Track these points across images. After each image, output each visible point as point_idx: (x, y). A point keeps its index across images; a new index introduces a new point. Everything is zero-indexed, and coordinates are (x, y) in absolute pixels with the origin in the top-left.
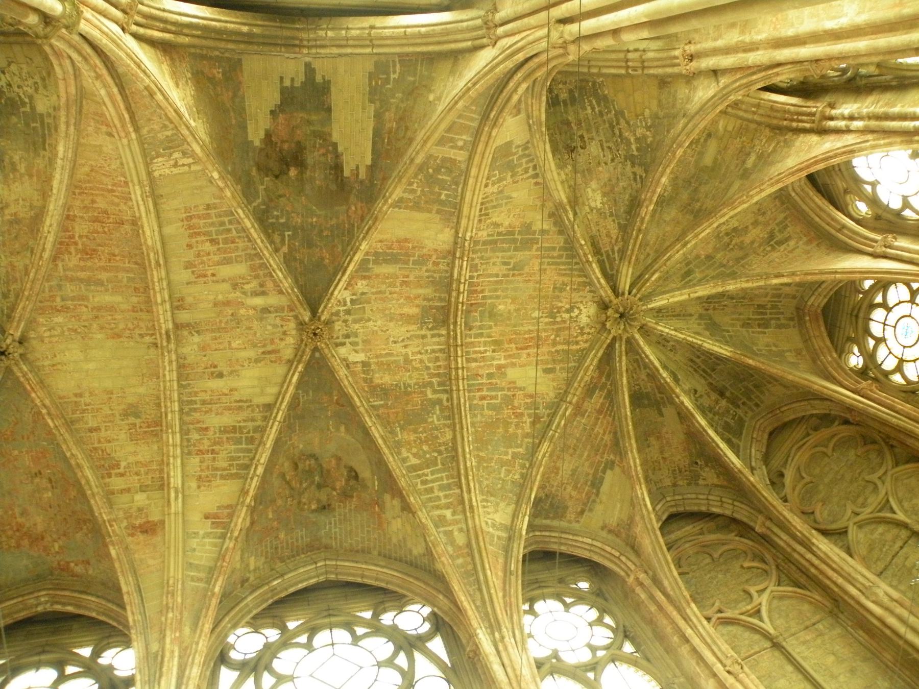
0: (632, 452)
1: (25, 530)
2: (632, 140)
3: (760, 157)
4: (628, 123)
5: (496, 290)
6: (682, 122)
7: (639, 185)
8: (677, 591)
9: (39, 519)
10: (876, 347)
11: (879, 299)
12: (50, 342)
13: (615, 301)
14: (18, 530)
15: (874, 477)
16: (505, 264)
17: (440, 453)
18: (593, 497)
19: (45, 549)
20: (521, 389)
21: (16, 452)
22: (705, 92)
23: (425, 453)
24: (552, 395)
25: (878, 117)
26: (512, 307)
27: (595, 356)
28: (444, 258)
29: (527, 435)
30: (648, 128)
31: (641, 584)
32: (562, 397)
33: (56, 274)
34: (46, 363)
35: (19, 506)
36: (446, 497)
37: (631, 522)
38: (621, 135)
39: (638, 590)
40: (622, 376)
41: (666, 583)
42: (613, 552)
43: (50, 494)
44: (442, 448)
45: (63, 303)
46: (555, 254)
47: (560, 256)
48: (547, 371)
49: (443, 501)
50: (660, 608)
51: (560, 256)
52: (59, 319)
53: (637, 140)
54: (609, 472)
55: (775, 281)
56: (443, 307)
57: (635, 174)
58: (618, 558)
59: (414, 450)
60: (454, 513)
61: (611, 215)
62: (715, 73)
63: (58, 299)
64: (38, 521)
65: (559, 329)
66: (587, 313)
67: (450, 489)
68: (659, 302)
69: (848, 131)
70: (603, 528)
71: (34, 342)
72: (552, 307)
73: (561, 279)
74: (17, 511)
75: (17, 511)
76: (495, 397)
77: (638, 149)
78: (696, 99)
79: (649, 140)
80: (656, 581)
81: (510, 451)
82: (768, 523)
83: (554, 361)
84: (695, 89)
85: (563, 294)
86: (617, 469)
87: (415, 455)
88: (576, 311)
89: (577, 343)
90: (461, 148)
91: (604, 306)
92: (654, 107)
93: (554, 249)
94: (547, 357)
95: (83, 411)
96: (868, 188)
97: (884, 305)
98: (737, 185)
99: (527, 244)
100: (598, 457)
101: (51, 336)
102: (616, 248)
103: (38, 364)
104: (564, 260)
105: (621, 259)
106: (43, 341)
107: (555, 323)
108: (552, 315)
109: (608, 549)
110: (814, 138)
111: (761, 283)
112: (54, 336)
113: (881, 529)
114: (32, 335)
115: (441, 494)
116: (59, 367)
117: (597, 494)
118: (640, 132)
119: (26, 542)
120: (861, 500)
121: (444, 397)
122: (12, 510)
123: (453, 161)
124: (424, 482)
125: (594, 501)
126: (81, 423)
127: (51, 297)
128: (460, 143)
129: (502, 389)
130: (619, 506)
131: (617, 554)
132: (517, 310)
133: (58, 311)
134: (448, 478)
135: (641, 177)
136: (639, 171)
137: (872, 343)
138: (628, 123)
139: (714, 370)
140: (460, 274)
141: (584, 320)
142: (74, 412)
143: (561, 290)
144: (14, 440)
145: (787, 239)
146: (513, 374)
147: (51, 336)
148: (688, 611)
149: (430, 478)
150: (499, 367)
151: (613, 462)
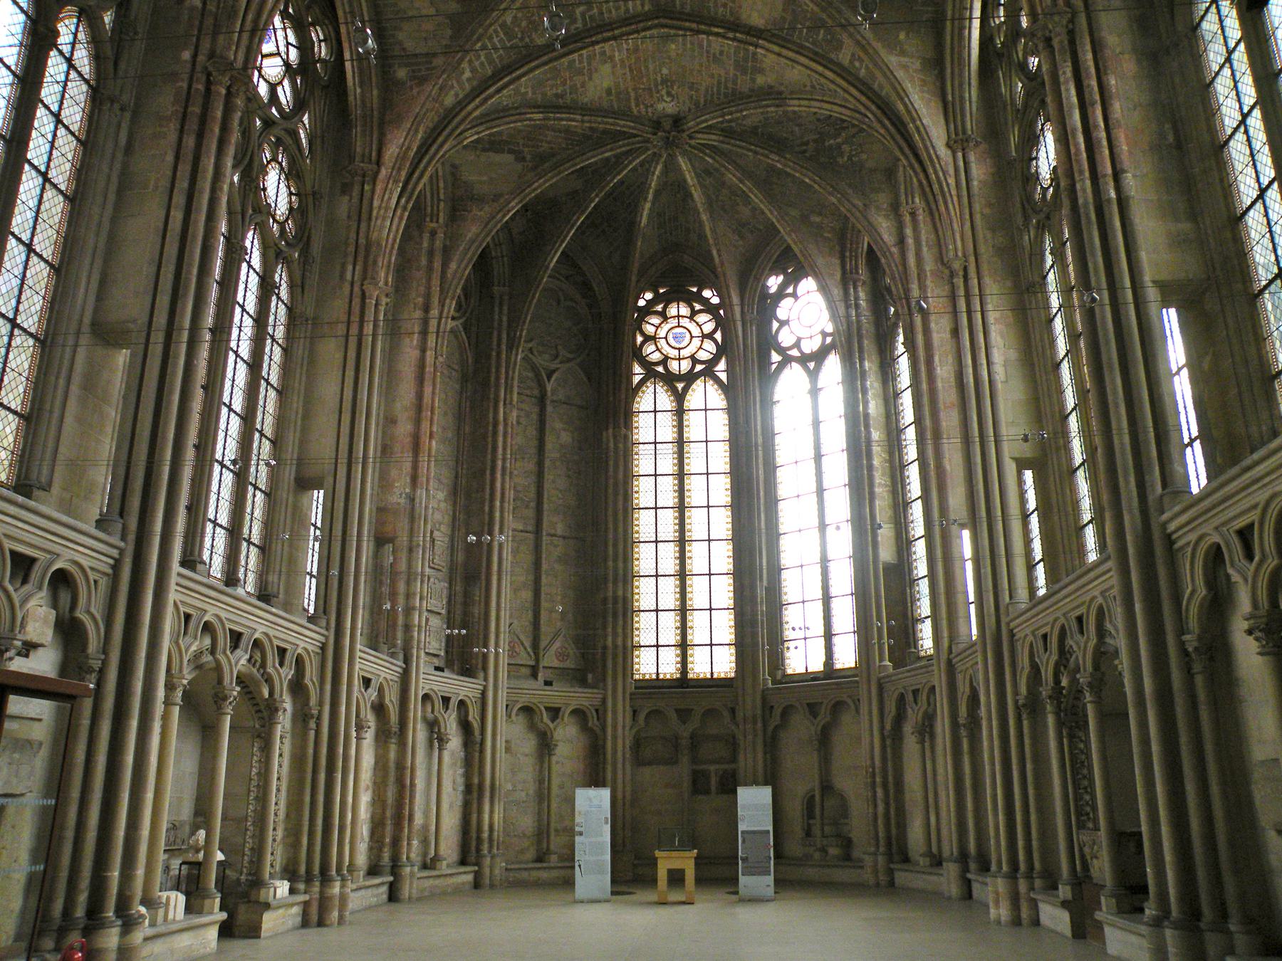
0: (545, 182)
2: (839, 140)
3: (820, 227)
4: (854, 136)
5: (692, 44)
6: (860, 204)
7: (797, 149)
8: (455, 282)
10: (657, 313)
11: (698, 307)
13: (685, 135)
15: (563, 352)
16: (721, 53)
17: (522, 39)
18: (480, 146)
20: (590, 79)
22: (885, 227)
23: (519, 26)
24: (586, 100)
25: (859, 329)
26: (673, 54)
27: (630, 127)
28: (732, 14)
29: (544, 94)
30: (850, 158)
31: (433, 233)
32: (586, 110)
36: (482, 64)
37: (481, 200)
38: (844, 128)
39: (426, 236)
40: (611, 150)
41: (453, 266)
42: (442, 191)
44: (527, 40)
46: (730, 85)
47: (726, 88)
48: (609, 92)
49: (477, 63)
50: (430, 268)
51: (726, 88)
53: (839, 146)
54: (509, 158)
55: (715, 252)
56: (674, 6)
57: (807, 144)
58: (439, 200)
59: (520, 15)
60: (469, 80)
61: (766, 119)
62: (901, 241)
65: (650, 89)
66: (668, 107)
67: (490, 64)
68: (683, 163)
69: (848, 307)
70: (454, 166)
72: (673, 82)
73: (703, 88)
76: (580, 62)
77: (831, 146)
78: (880, 220)
79: (840, 160)
80: (447, 252)
81: (529, 90)
82: (506, 297)
83: (618, 94)
84: (887, 217)
85: (687, 90)
86: (519, 167)
87: (515, 17)
88: (668, 99)
89: (637, 105)
90: (851, 62)
91: (677, 121)
92: (870, 164)
93: (735, 83)
94: (622, 86)
96: (790, 290)
97: (694, 313)
98: (794, 213)
99: (741, 67)
100: (521, 142)
102: (733, 124)
104: (722, 90)
105: (722, 130)
107: (656, 86)
108: (664, 81)
109: (441, 185)
110: (838, 276)
111: (711, 241)
113: (530, 375)
115: (483, 58)
117: (484, 150)
118: (846, 148)
120: (541, 349)
121: (579, 24)
123: (839, 46)
124: (490, 38)
125: (476, 148)
128: (857, 64)
129: (589, 64)
130: (485, 178)
131: (442, 197)
132: (669, 58)
134: (500, 57)
135: (805, 151)
136: (812, 146)
137: (659, 308)
138: (854, 136)
139: (615, 199)
140: (717, 34)
141: (660, 106)
143: (691, 88)
145: (742, 237)
146: (606, 69)
148: (448, 301)
149: (495, 40)
150: (611, 58)
151: (524, 159)
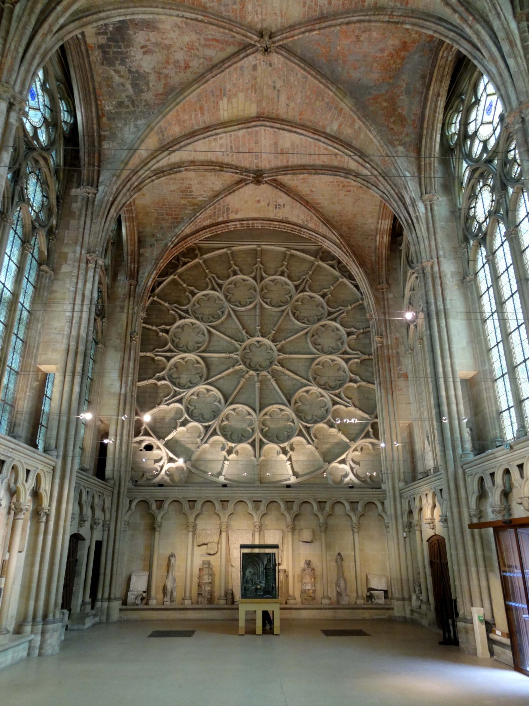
1: (394, 53)
9: (390, 42)
12: (266, 14)
14: (392, 57)
19: (414, 42)
21: (339, 48)
33: (216, 7)
34: (279, 20)
35: (376, 52)
43: (374, 33)
45: (238, 4)
52: (250, 7)
63: (235, 7)
64: (393, 42)
71: (265, 25)
74: (379, 54)
75: (379, 54)
95: (316, 4)
101: (262, 14)
103: (279, 25)
106: (264, 20)
112: (262, 12)
114: (259, 26)
116: (283, 13)
119: (403, 54)
122: (377, 57)
126: (323, 8)
127: (233, 11)
133: (243, 7)
142: (315, 11)
144: (329, 48)
147: (262, 14)
